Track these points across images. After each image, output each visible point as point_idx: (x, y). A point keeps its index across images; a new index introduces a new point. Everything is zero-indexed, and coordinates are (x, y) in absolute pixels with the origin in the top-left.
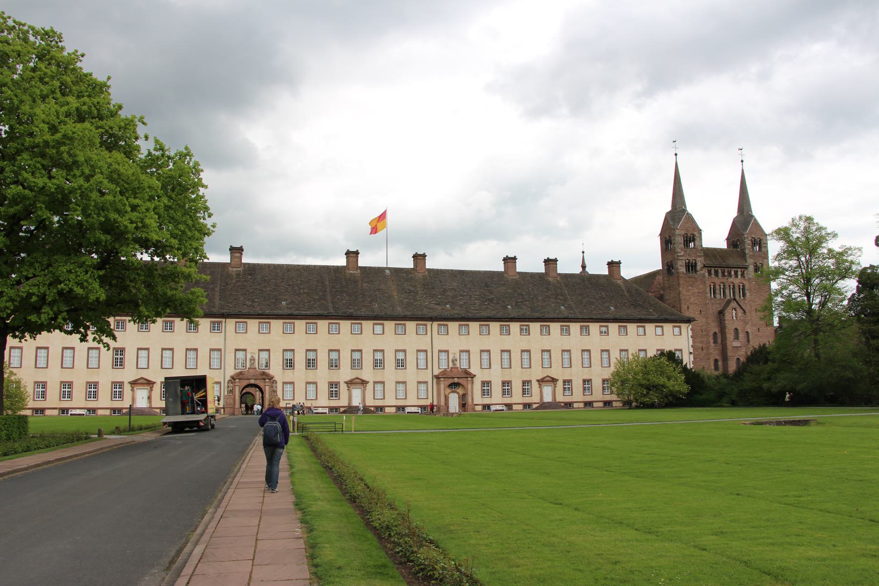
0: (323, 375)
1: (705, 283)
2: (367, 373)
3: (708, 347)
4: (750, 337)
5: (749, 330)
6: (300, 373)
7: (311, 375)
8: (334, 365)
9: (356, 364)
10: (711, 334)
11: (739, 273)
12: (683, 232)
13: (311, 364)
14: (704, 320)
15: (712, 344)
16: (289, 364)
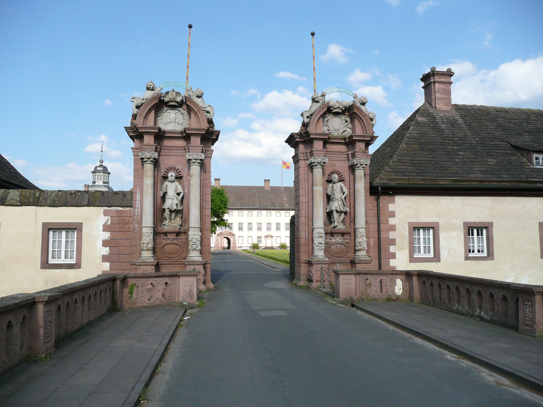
0: (255, 233)
2: (273, 232)
6: (245, 232)
7: (250, 233)
8: (259, 229)
9: (269, 229)
13: (250, 229)
16: (241, 229)
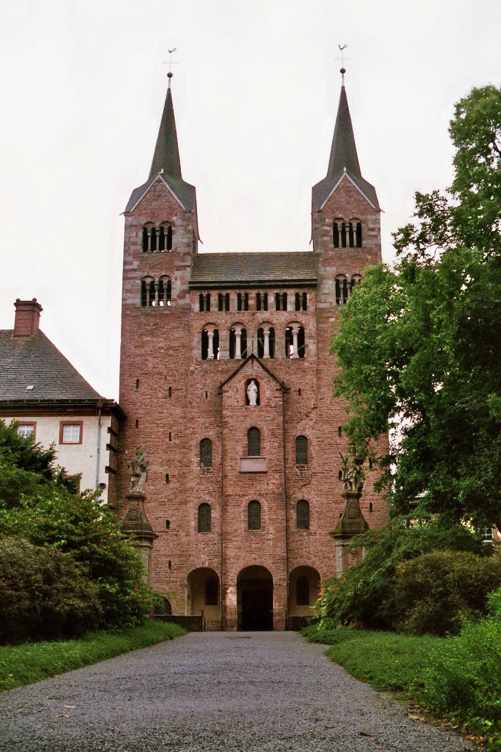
1: (188, 327)
3: (183, 476)
4: (313, 450)
5: (308, 433)
10: (195, 442)
11: (291, 299)
12: (143, 220)
14: (178, 411)
15: (195, 467)
